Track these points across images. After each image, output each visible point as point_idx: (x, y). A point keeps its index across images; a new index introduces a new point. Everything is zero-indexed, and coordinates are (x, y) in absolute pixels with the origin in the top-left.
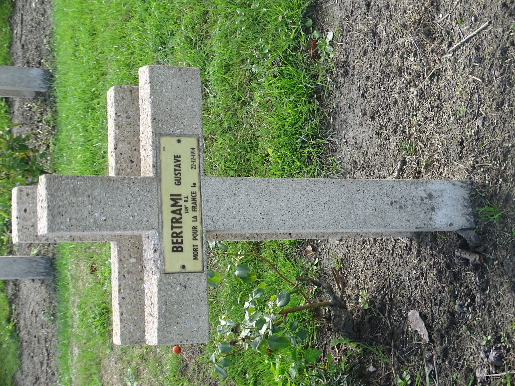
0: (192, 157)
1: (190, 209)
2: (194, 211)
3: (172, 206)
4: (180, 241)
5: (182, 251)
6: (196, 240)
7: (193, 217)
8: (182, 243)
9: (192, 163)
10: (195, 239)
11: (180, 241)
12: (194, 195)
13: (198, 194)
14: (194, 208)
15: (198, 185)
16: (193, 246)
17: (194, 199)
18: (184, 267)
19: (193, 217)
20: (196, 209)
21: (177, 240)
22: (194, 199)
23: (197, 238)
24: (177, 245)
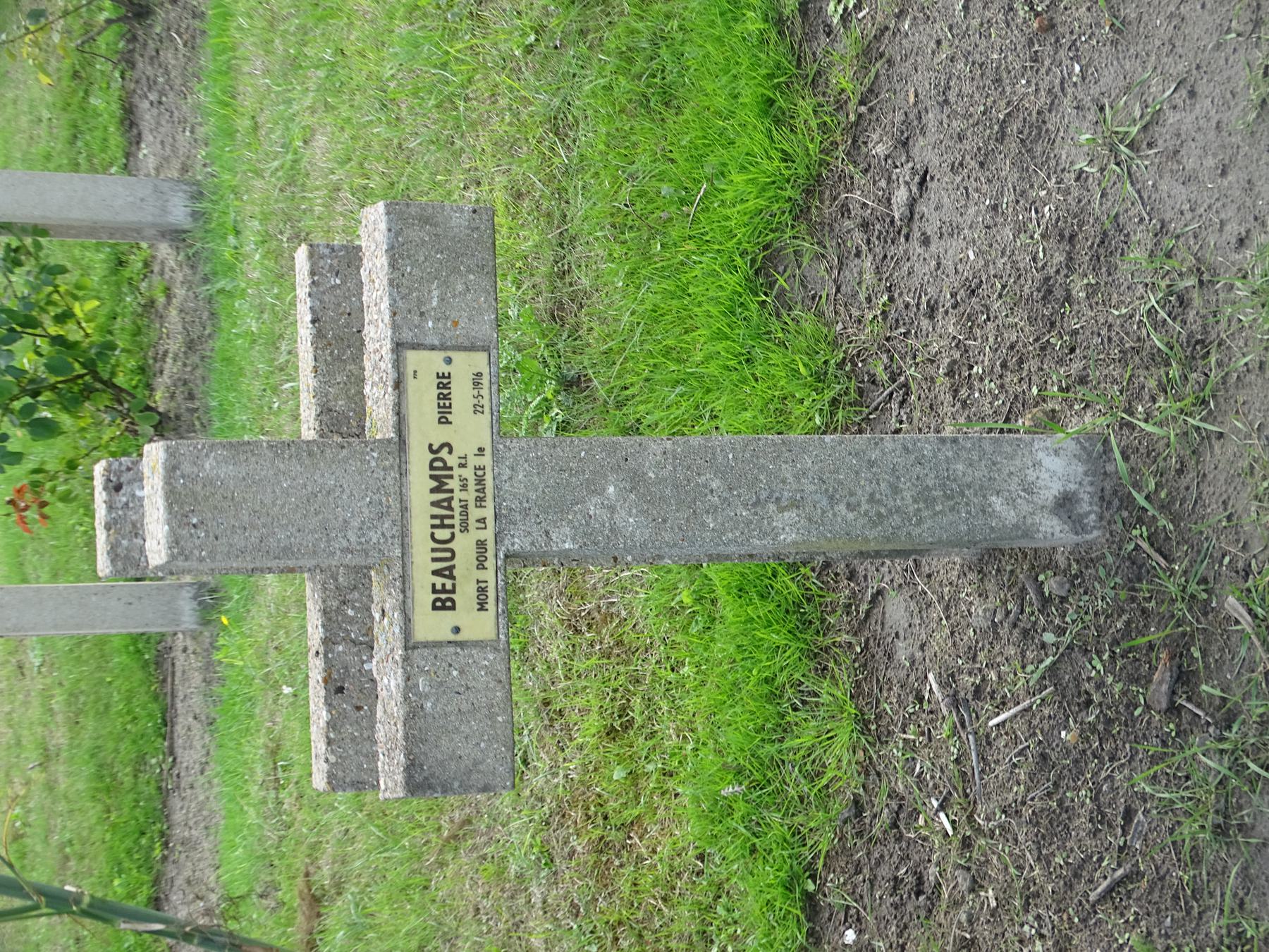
1: (471, 504)
3: (433, 491)
6: (484, 568)
7: (478, 521)
8: (453, 591)
10: (481, 566)
11: (449, 587)
12: (480, 473)
14: (480, 501)
15: (488, 452)
16: (478, 582)
17: (480, 481)
19: (478, 521)
21: (444, 585)
22: (480, 481)
23: (486, 564)
24: (443, 596)
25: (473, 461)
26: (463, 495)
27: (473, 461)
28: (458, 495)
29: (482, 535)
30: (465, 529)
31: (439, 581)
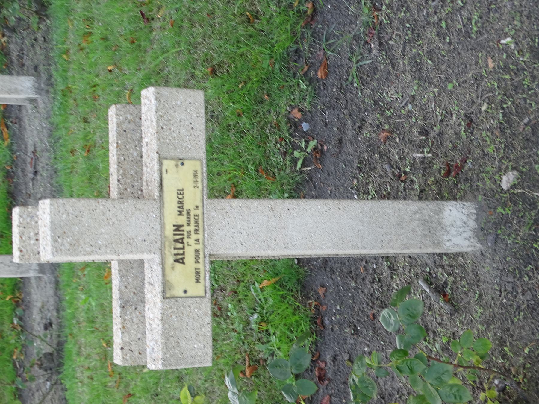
0: (195, 180)
2: (197, 233)
6: (199, 262)
7: (196, 240)
9: (195, 185)
10: (197, 262)
12: (196, 218)
13: (201, 217)
14: (196, 231)
15: (200, 208)
16: (196, 269)
17: (196, 222)
19: (196, 240)
22: (196, 222)
23: (199, 261)
25: (192, 213)
28: (186, 228)
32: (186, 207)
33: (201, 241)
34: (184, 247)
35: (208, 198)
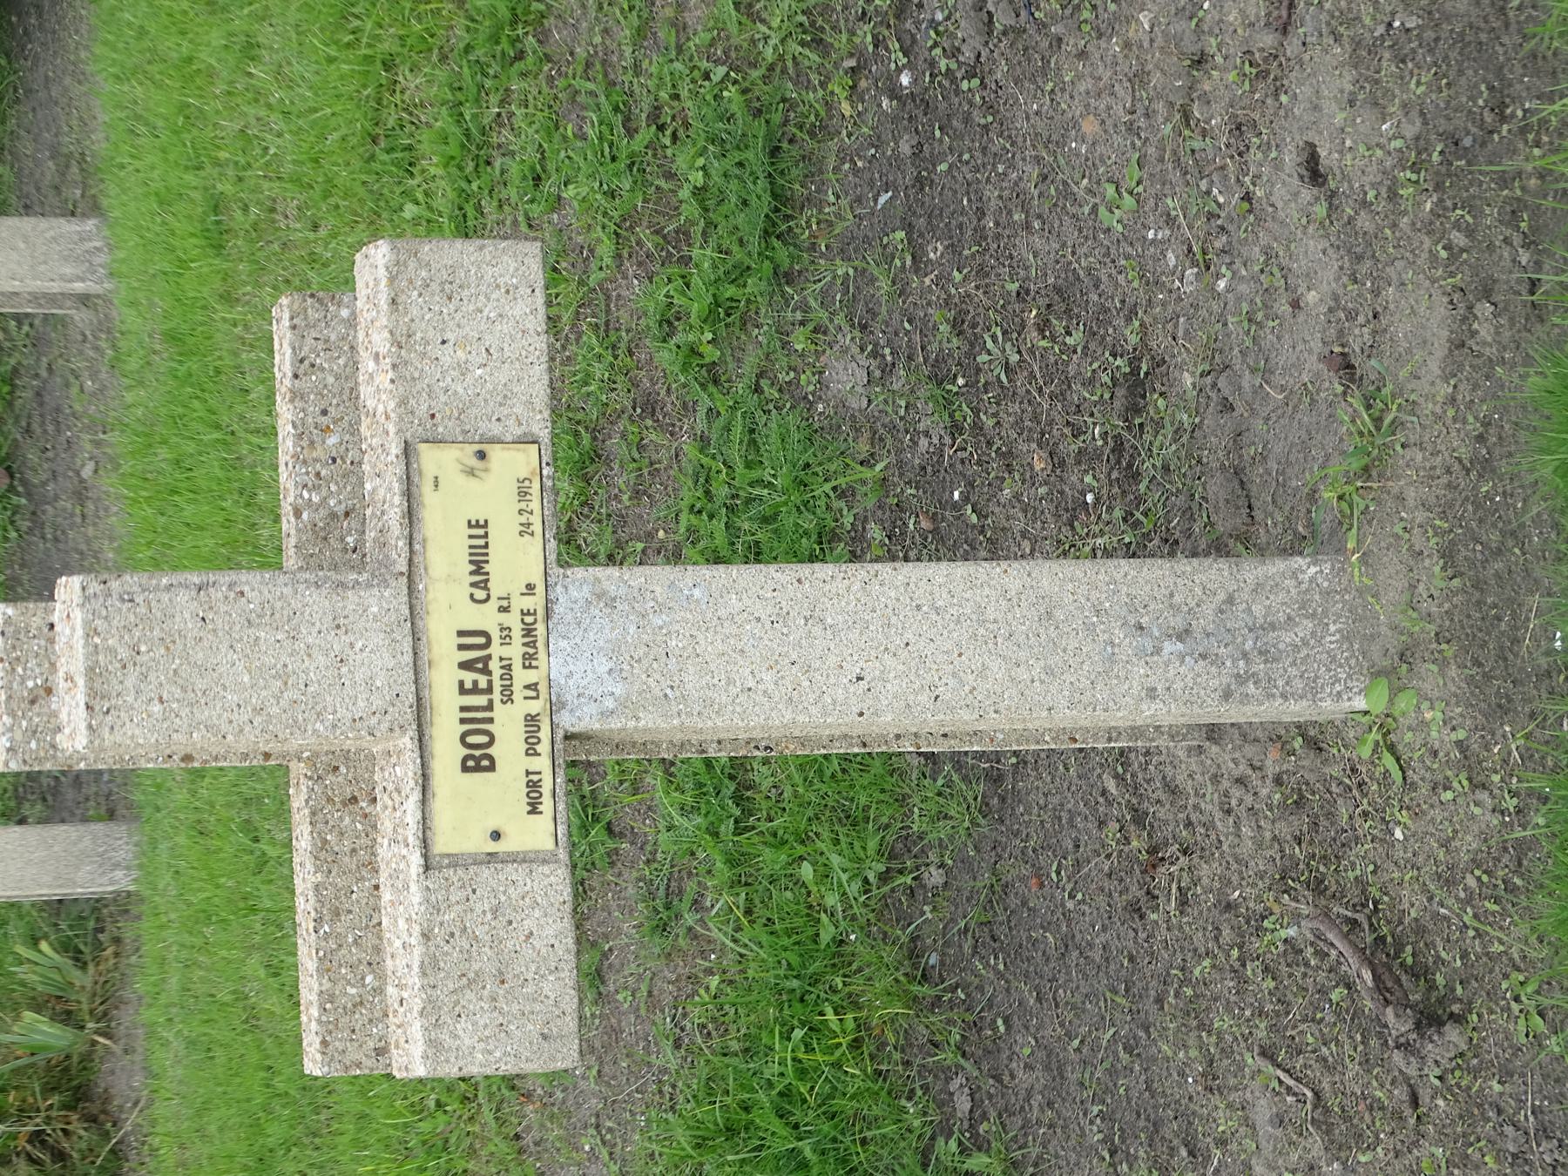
0: (523, 505)
2: (530, 667)
4: (483, 684)
5: (492, 768)
7: (527, 687)
10: (531, 752)
11: (483, 684)
12: (529, 619)
14: (529, 661)
15: (540, 589)
16: (528, 773)
17: (529, 631)
18: (496, 836)
19: (527, 687)
20: (534, 663)
23: (539, 748)
26: (506, 652)
27: (520, 603)
28: (496, 650)
29: (535, 707)
30: (508, 698)
31: (469, 677)
32: (496, 589)
33: (543, 688)
34: (490, 683)
35: (563, 564)
